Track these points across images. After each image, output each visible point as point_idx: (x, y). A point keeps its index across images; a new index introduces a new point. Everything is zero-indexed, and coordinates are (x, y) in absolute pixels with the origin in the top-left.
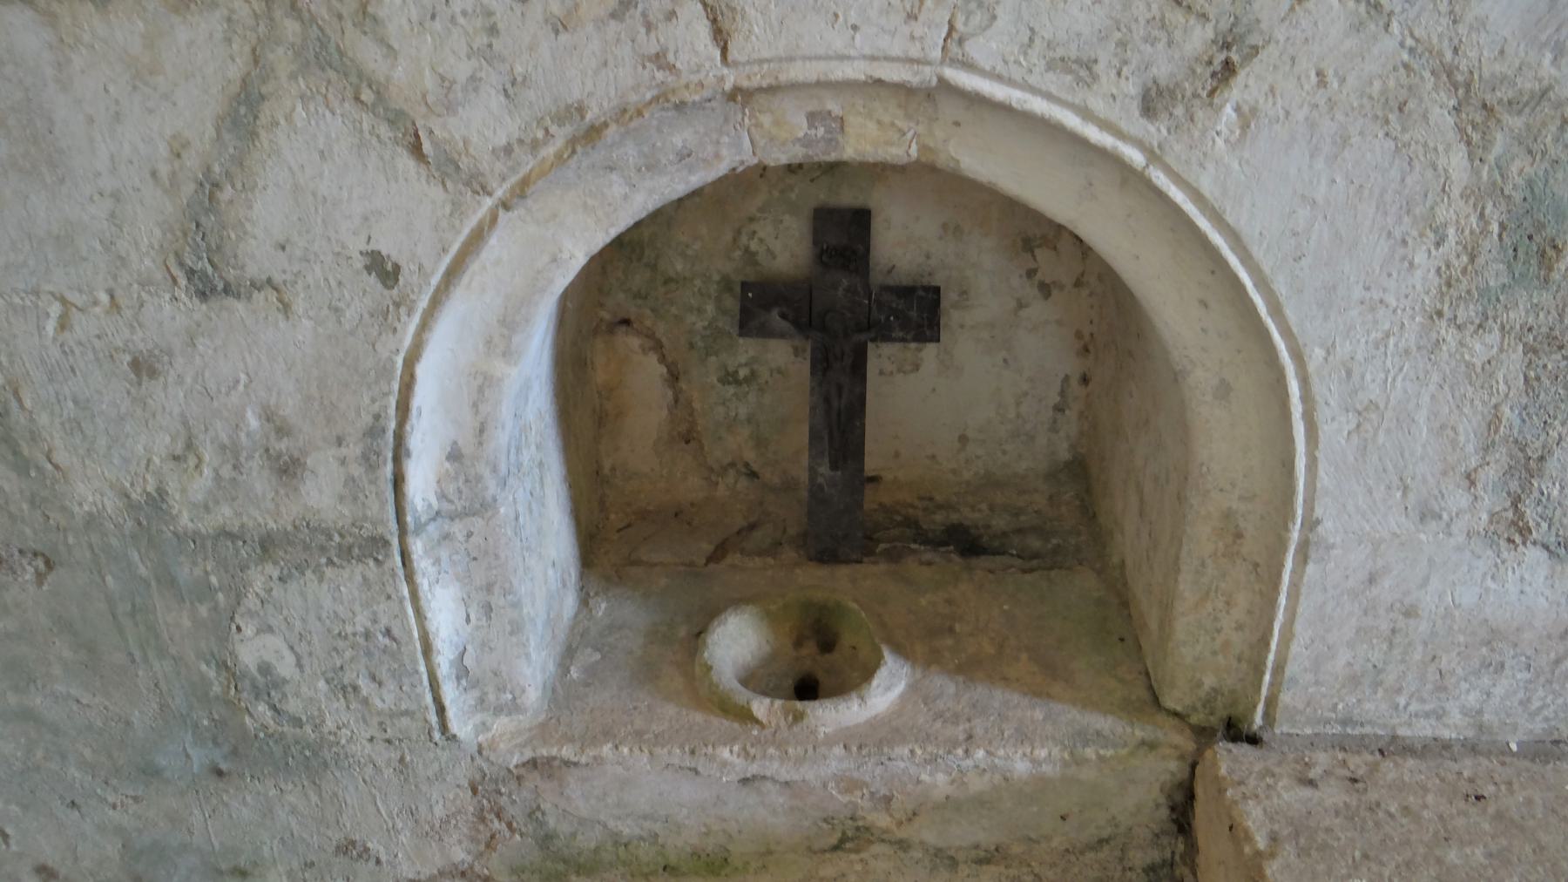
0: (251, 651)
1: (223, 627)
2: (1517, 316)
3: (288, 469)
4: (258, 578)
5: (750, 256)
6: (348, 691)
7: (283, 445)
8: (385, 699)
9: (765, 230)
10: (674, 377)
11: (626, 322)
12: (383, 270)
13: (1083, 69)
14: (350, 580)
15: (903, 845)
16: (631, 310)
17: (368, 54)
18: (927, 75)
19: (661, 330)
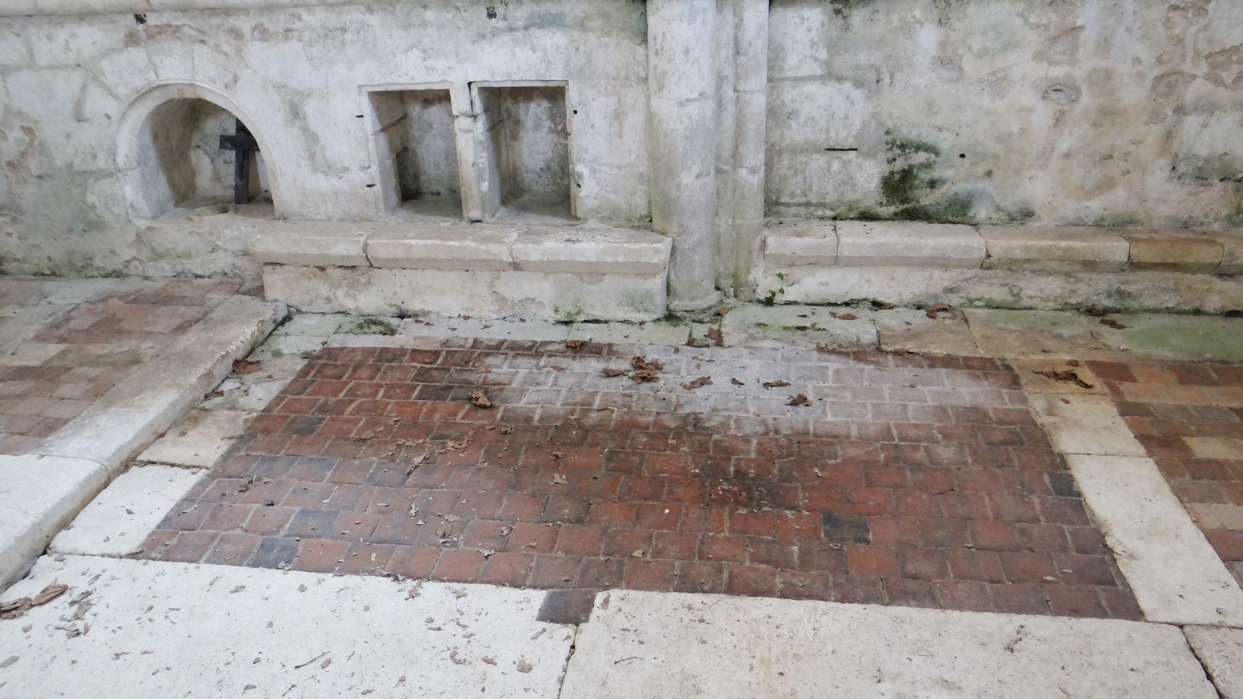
0: (91, 198)
1: (84, 193)
2: (298, 125)
3: (94, 157)
4: (91, 181)
5: (225, 129)
6: (108, 208)
7: (93, 152)
8: (116, 211)
9: (227, 123)
10: (212, 162)
11: (199, 146)
12: (108, 117)
13: (214, 81)
14: (107, 181)
15: (225, 250)
16: (200, 143)
17: (102, 78)
18: (191, 82)
19: (207, 148)
